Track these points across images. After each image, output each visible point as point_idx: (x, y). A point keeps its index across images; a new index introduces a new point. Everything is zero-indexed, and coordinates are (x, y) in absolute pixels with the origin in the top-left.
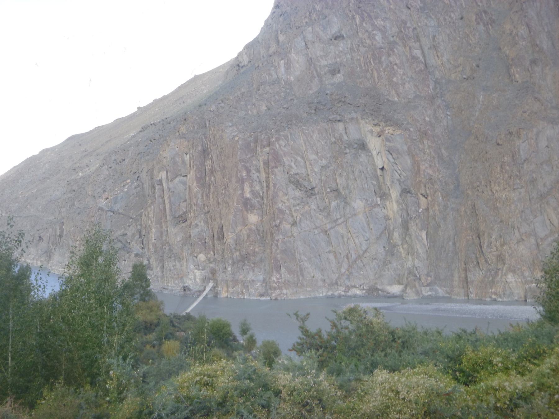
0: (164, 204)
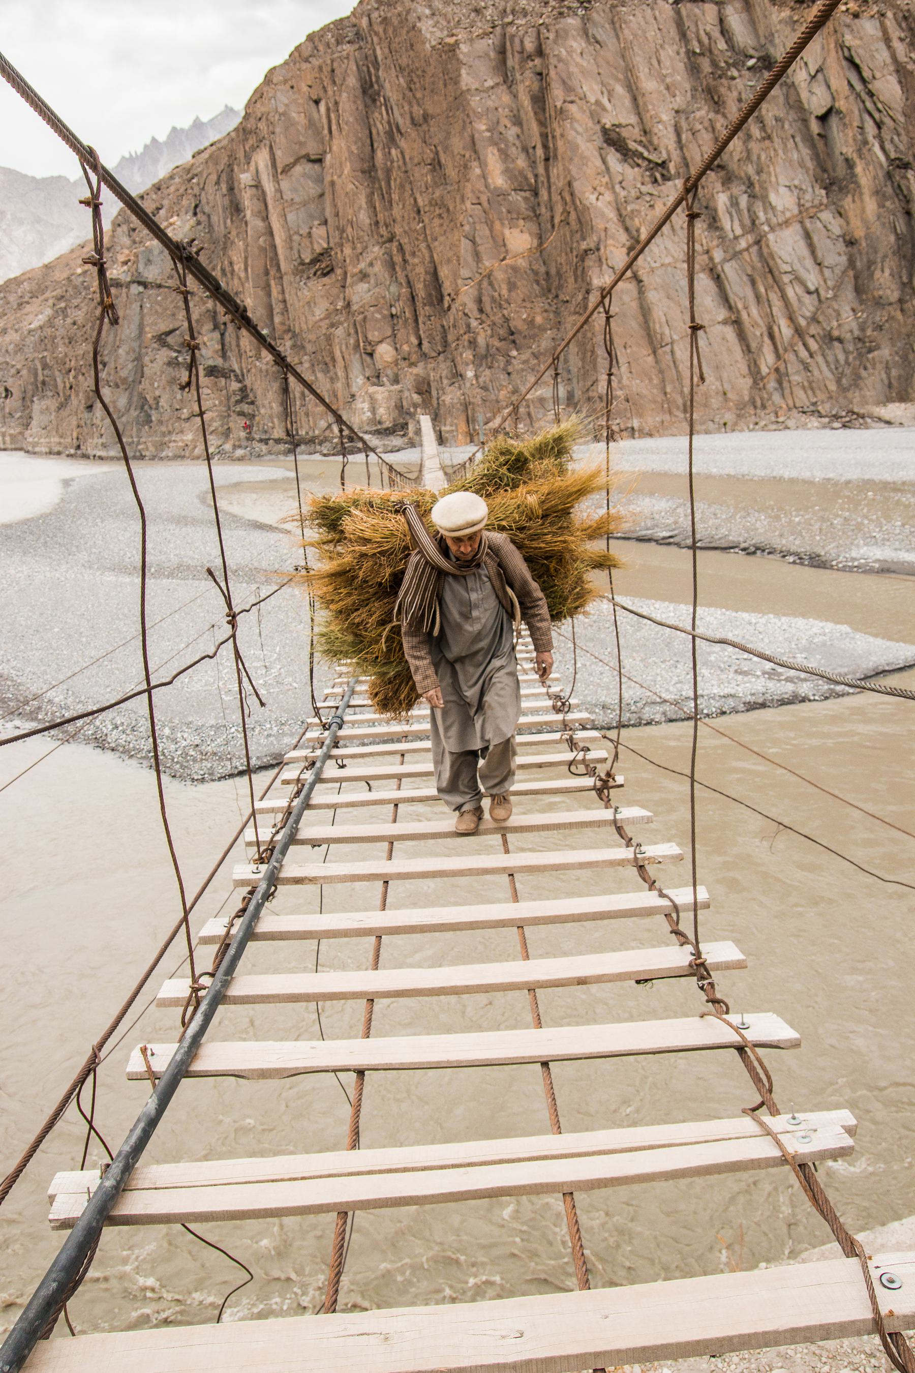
0: (271, 234)
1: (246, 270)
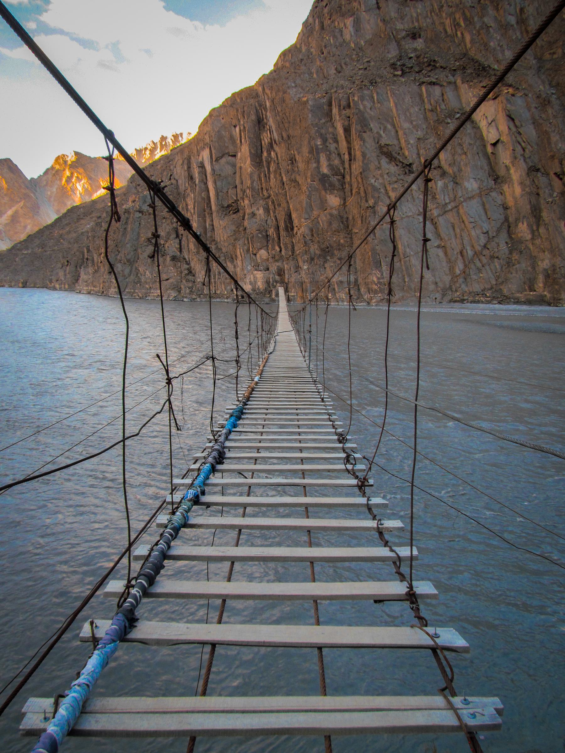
0: (208, 191)
1: (194, 208)
